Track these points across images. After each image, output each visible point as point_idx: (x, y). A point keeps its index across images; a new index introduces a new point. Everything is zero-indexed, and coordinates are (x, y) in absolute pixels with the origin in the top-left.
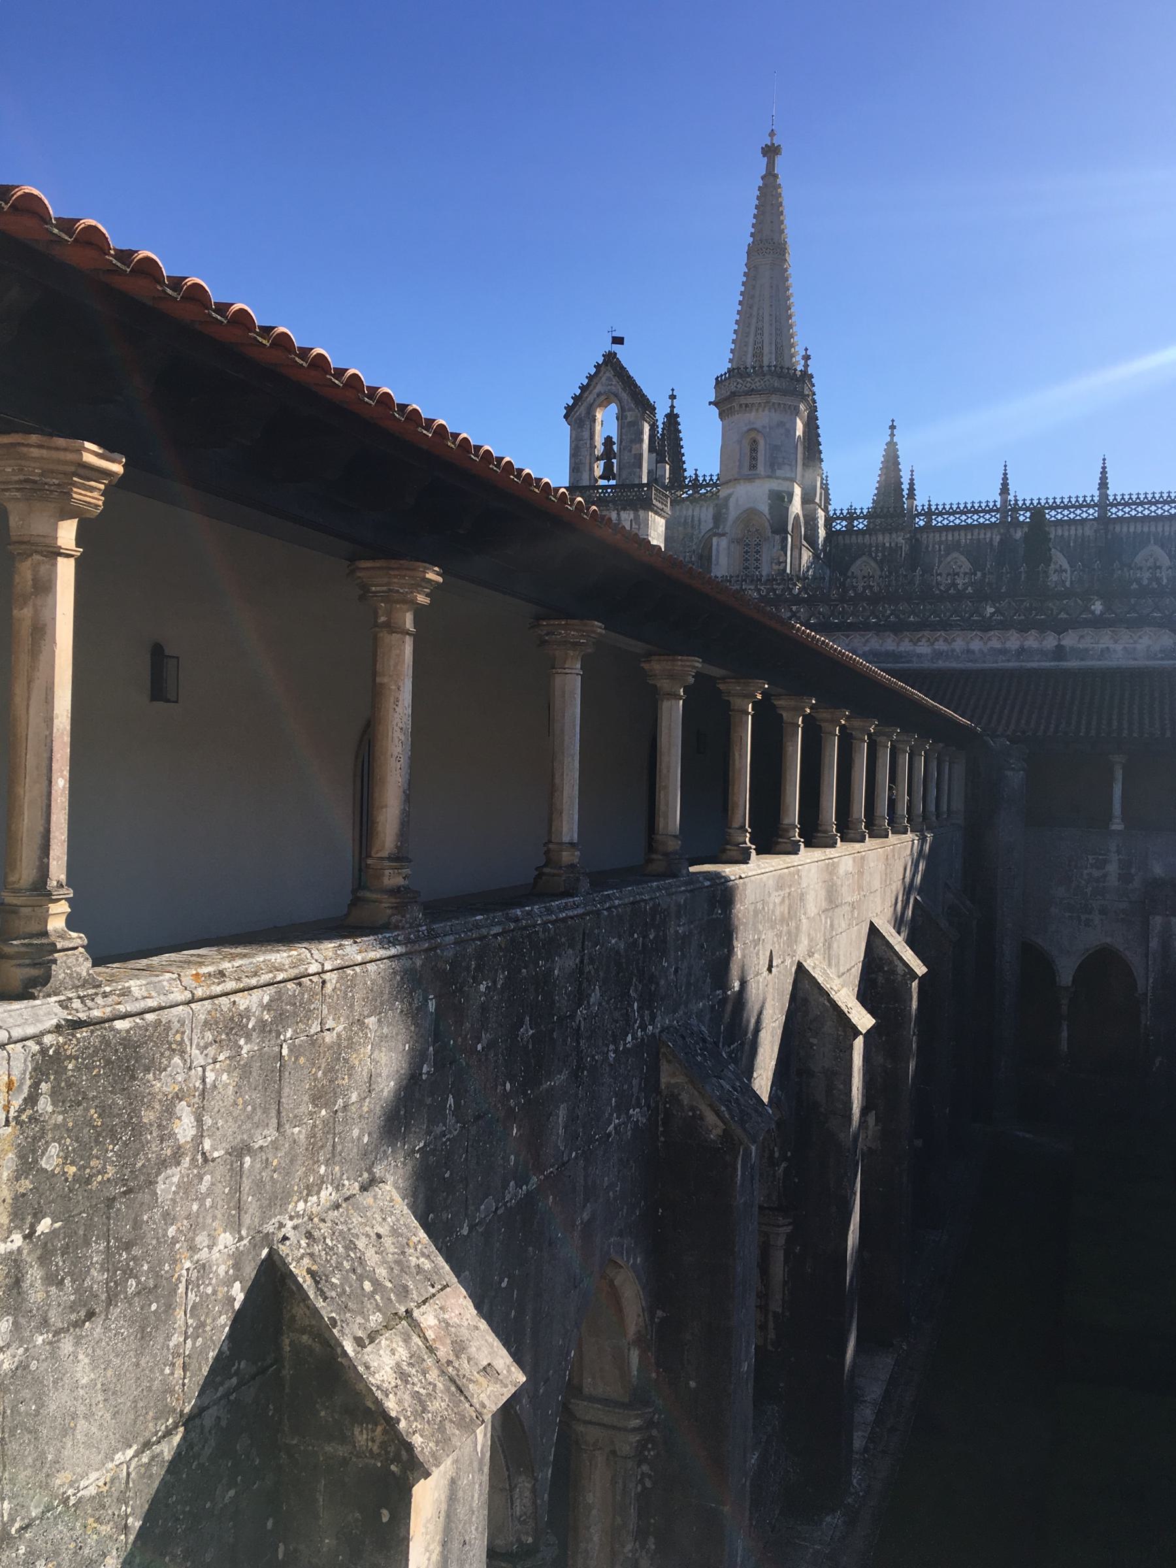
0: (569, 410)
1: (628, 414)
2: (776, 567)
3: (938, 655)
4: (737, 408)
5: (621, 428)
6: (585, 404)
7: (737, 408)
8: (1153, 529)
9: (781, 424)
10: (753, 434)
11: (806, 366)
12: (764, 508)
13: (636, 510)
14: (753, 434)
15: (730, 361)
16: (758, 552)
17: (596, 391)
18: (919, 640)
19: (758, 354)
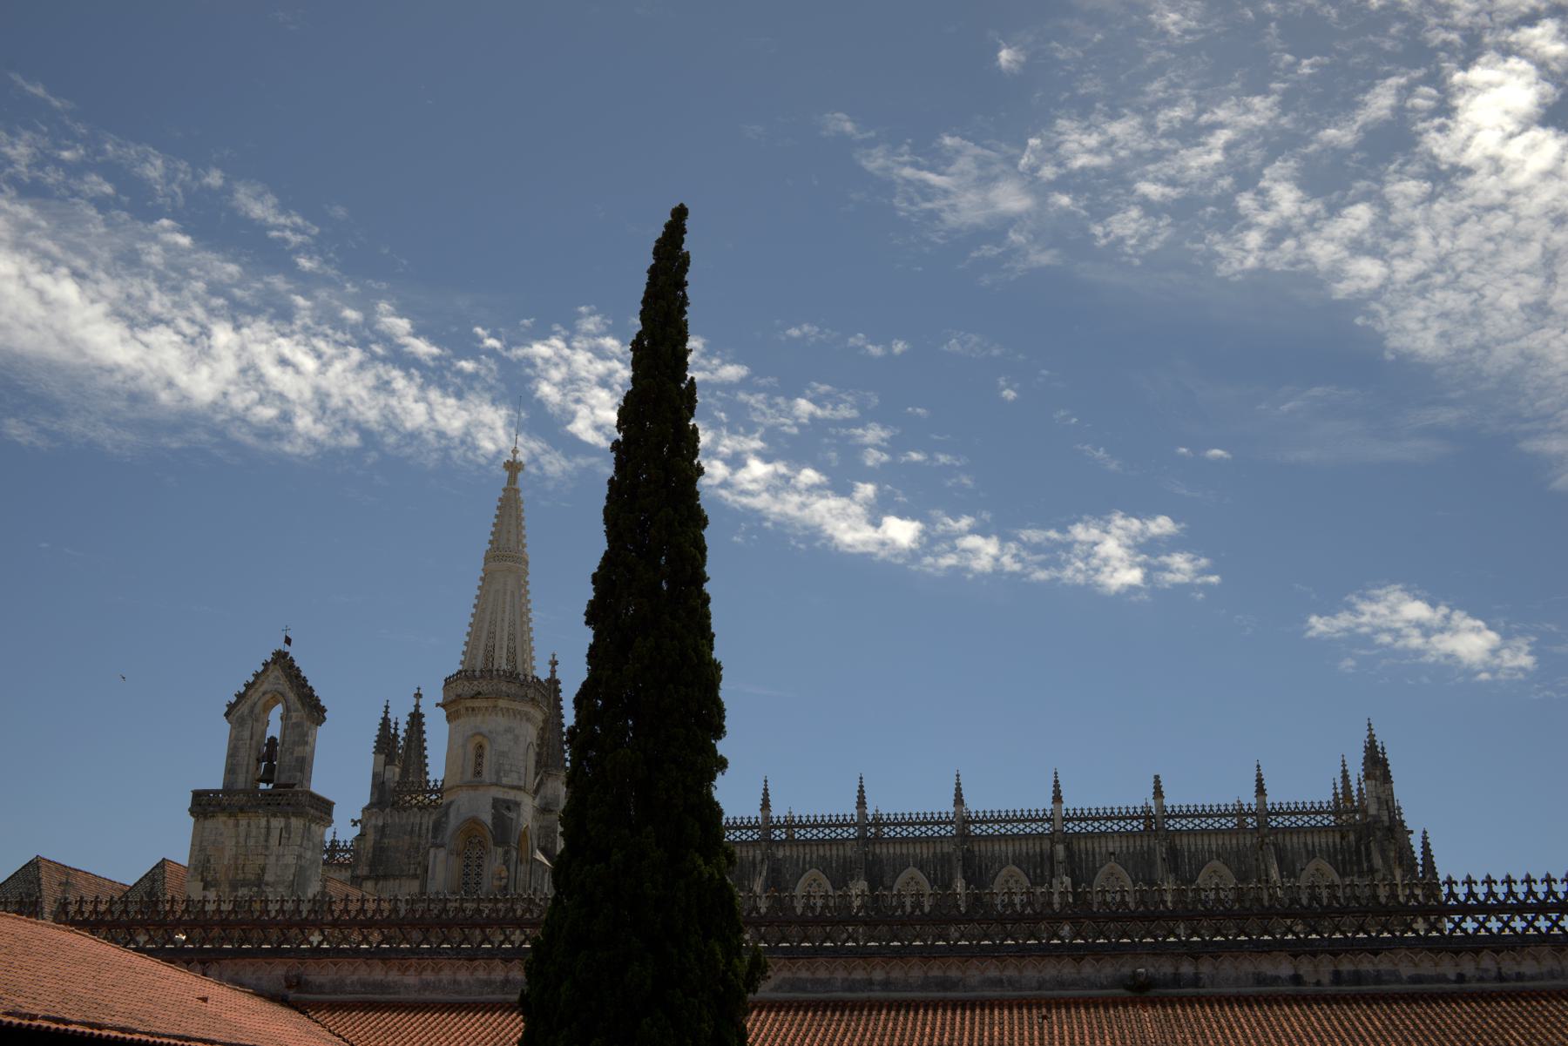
0: (232, 708)
1: (294, 714)
2: (496, 883)
3: (426, 986)
4: (463, 711)
5: (284, 728)
6: (249, 702)
7: (463, 711)
8: (911, 850)
9: (509, 730)
10: (479, 739)
11: (553, 672)
12: (487, 817)
13: (287, 816)
14: (479, 739)
15: (462, 663)
16: (479, 866)
17: (262, 689)
18: (407, 969)
19: (489, 655)
